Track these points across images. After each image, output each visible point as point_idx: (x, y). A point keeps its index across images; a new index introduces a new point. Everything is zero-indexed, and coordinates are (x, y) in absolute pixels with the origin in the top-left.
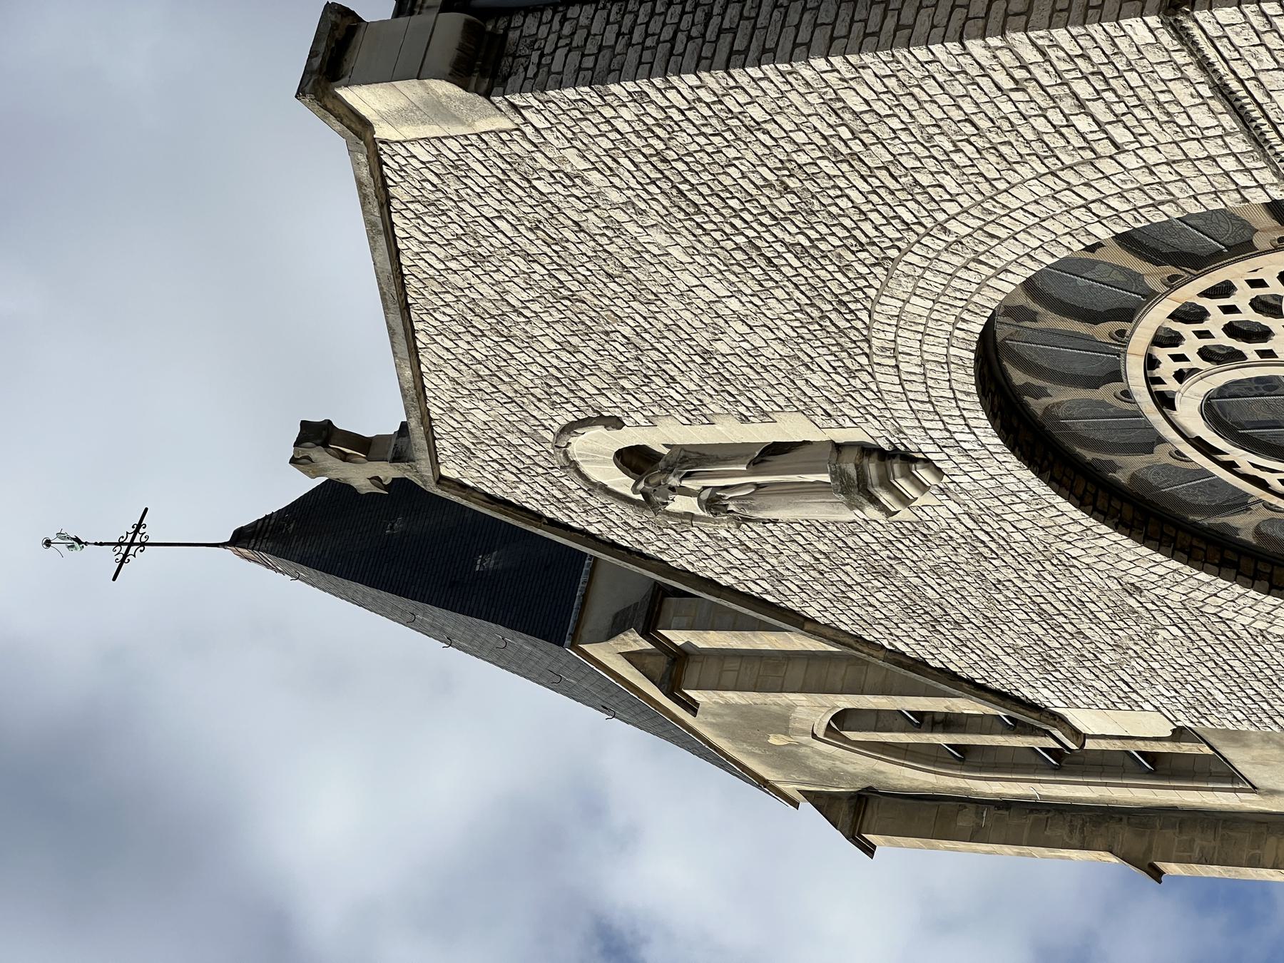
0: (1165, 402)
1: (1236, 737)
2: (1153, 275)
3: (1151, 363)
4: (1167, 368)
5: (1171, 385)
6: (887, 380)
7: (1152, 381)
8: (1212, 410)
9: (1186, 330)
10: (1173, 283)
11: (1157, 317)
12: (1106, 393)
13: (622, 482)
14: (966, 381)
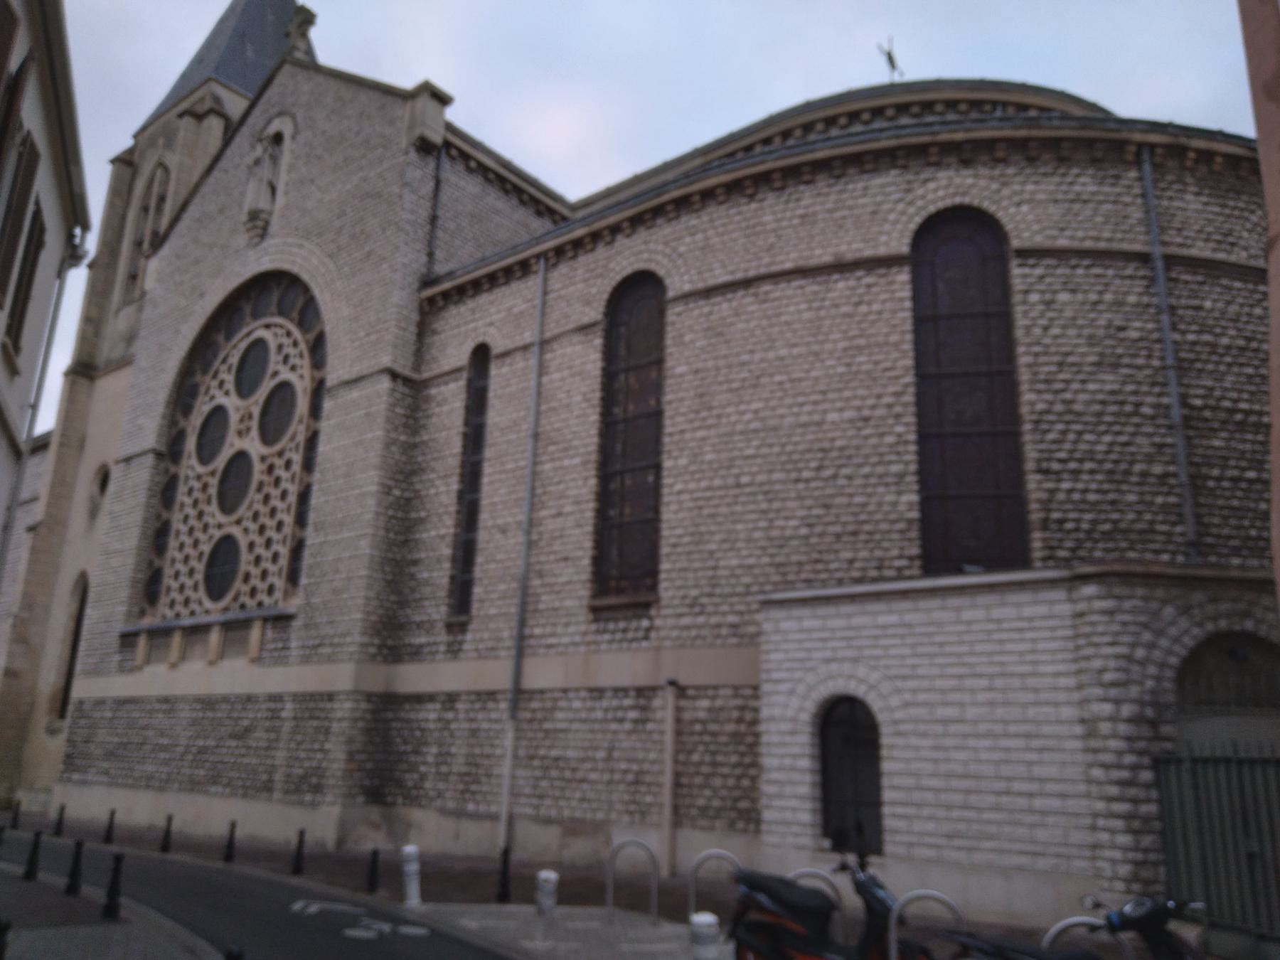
0: (268, 326)
1: (140, 309)
2: (311, 336)
3: (281, 327)
4: (279, 331)
5: (274, 330)
6: (291, 240)
7: (276, 325)
8: (260, 342)
9: (290, 341)
10: (307, 342)
11: (297, 333)
12: (273, 308)
13: (272, 130)
14: (286, 266)
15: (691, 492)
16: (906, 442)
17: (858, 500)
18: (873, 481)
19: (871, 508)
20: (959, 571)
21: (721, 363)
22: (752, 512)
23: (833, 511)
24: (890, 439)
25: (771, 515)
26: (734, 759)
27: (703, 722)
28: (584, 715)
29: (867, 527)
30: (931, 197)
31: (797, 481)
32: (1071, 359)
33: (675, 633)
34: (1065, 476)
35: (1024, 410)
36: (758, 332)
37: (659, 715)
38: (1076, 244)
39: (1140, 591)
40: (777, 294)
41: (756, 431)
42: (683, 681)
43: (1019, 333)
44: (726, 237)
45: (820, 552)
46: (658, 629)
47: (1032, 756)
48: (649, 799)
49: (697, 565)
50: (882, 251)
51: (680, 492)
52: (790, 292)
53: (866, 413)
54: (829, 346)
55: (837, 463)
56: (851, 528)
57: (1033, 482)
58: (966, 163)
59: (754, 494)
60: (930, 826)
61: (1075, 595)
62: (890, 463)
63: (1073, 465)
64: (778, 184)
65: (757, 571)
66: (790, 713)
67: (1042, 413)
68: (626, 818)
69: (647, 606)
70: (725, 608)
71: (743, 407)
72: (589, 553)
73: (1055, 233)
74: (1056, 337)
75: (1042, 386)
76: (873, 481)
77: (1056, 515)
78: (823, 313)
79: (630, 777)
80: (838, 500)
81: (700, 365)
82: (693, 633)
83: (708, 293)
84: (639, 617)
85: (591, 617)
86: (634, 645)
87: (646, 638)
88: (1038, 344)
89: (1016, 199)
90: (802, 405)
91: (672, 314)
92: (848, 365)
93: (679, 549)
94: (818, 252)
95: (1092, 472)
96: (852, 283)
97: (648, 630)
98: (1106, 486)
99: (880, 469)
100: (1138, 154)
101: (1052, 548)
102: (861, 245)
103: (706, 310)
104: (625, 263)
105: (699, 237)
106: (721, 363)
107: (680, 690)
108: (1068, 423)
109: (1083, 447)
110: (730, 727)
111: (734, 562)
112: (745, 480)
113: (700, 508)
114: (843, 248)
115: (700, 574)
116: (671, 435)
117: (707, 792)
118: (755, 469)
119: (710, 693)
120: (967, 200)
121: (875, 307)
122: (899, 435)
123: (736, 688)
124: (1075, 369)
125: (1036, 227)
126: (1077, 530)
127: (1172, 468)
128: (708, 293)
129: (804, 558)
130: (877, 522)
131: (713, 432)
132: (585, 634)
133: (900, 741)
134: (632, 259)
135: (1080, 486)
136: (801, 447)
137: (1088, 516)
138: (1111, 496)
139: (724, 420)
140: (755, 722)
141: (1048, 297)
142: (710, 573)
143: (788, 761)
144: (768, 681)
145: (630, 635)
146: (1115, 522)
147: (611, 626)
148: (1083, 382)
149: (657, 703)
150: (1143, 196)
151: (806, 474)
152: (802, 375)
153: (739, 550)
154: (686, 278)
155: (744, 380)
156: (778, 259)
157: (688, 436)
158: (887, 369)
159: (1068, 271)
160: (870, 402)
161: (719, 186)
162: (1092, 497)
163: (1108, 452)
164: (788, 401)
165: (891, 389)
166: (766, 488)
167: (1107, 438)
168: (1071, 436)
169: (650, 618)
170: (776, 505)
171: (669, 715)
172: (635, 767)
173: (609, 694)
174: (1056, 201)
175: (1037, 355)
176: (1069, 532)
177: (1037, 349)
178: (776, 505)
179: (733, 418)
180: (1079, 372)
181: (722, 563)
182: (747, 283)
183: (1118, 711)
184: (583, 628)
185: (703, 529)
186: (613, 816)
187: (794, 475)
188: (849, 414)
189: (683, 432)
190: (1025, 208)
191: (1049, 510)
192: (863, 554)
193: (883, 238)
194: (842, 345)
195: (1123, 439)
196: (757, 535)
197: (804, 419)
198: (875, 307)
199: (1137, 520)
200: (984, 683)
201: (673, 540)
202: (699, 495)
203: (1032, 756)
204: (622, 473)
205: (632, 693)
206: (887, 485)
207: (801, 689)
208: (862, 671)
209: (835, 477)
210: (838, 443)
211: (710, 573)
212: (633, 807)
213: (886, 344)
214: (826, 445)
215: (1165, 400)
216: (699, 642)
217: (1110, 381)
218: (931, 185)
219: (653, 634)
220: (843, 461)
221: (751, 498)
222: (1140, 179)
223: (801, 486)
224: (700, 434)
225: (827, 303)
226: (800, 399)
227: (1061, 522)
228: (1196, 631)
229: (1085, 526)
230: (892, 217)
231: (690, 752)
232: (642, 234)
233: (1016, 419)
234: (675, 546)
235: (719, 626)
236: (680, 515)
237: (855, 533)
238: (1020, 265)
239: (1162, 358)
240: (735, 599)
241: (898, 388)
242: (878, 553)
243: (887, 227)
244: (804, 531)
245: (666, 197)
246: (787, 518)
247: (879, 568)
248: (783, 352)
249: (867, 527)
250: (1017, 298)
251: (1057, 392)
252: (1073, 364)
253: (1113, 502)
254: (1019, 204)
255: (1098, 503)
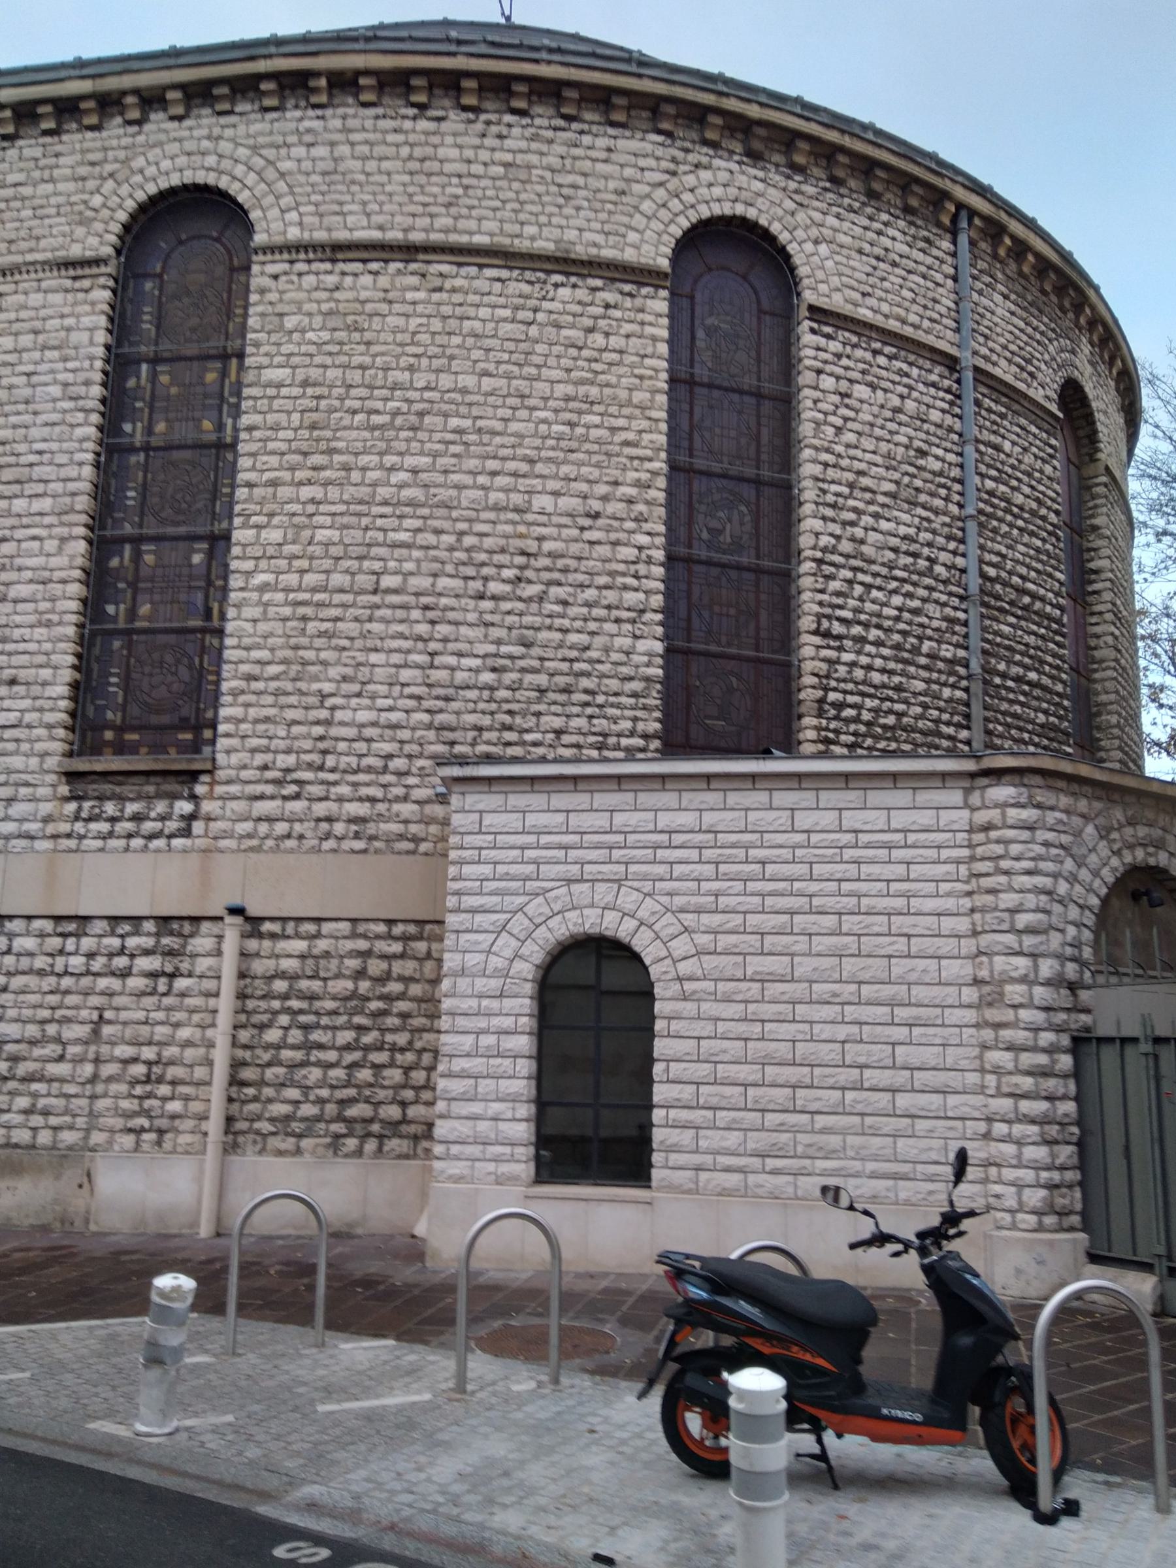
15: (287, 590)
16: (649, 561)
17: (573, 638)
18: (598, 612)
19: (593, 654)
20: (766, 753)
21: (356, 376)
22: (402, 636)
23: (536, 651)
24: (628, 553)
25: (433, 646)
26: (346, 1036)
27: (293, 977)
28: (40, 962)
29: (585, 683)
30: (703, 191)
31: (481, 597)
32: (865, 481)
33: (247, 826)
34: (848, 643)
35: (805, 541)
36: (424, 338)
37: (203, 964)
38: (879, 320)
39: (1064, 801)
40: (458, 282)
41: (410, 503)
42: (253, 910)
43: (806, 429)
44: (371, 166)
45: (510, 712)
46: (209, 819)
47: (901, 1033)
48: (175, 1106)
49: (290, 714)
50: (629, 255)
51: (263, 588)
52: (481, 284)
53: (596, 505)
54: (542, 387)
55: (546, 576)
56: (561, 680)
57: (808, 647)
58: (754, 157)
59: (405, 607)
60: (733, 1139)
61: (975, 799)
62: (625, 588)
63: (857, 630)
64: (469, 100)
65: (405, 734)
66: (495, 962)
67: (824, 550)
68: (128, 1140)
69: (193, 776)
70: (345, 790)
71: (389, 460)
72: (67, 675)
73: (857, 296)
74: (848, 446)
75: (829, 512)
76: (598, 612)
77: (832, 696)
78: (533, 331)
79: (139, 1070)
80: (544, 635)
81: (315, 373)
82: (281, 828)
83: (336, 251)
84: (174, 797)
85: (64, 790)
86: (160, 843)
87: (186, 833)
88: (828, 451)
89: (814, 232)
90: (494, 474)
91: (261, 274)
92: (571, 424)
93: (259, 685)
94: (531, 230)
95: (878, 643)
96: (582, 294)
97: (192, 817)
98: (892, 665)
99: (611, 596)
100: (955, 219)
101: (827, 741)
102: (599, 239)
103: (331, 280)
104: (166, 164)
105: (321, 151)
106: (356, 376)
107: (253, 924)
108: (855, 569)
109: (869, 606)
110: (344, 986)
111: (363, 716)
112: (388, 581)
113: (304, 619)
114: (571, 235)
115: (296, 730)
116: (250, 485)
117: (293, 1093)
118: (409, 566)
119: (311, 928)
120: (751, 213)
121: (615, 342)
122: (640, 548)
123: (390, 922)
124: (868, 496)
125: (835, 281)
126: (857, 720)
127: (961, 653)
128: (336, 251)
129: (486, 721)
130: (603, 676)
131: (333, 493)
132: (47, 820)
133: (689, 1008)
134: (182, 161)
135: (864, 660)
136: (488, 542)
137: (869, 703)
138: (896, 679)
139: (355, 476)
140: (435, 982)
141: (844, 386)
142: (318, 730)
143: (488, 1040)
144: (457, 910)
145: (149, 826)
146: (900, 715)
147: (110, 808)
148: (876, 516)
149: (202, 943)
150: (955, 279)
151: (494, 587)
152: (498, 426)
153: (373, 697)
154: (293, 216)
155: (396, 413)
156: (462, 224)
157: (284, 492)
158: (627, 443)
159: (868, 356)
160: (602, 489)
161: (367, 72)
162: (876, 677)
163: (897, 619)
164: (472, 463)
165: (632, 475)
166: (424, 600)
167: (897, 600)
168: (858, 590)
169: (193, 797)
170: (443, 629)
171: (229, 965)
172: (148, 1053)
173: (99, 926)
174: (860, 252)
175: (826, 465)
176: (848, 721)
177: (825, 457)
178: (443, 629)
179: (372, 475)
180: (870, 502)
181: (339, 715)
182: (409, 251)
183: (1036, 967)
184: (46, 808)
185: (310, 655)
186: (97, 1138)
187: (477, 585)
188: (565, 503)
189: (274, 483)
190: (823, 249)
191: (826, 689)
192: (581, 722)
193: (633, 237)
194: (561, 390)
195: (916, 604)
196: (406, 675)
197: (494, 497)
198: (615, 342)
199: (922, 717)
200: (829, 921)
201: (244, 668)
202: (306, 596)
203: (901, 1033)
204: (137, 541)
205: (149, 926)
206: (617, 621)
207: (519, 924)
208: (628, 899)
209: (541, 599)
210: (548, 546)
211: (318, 730)
212: (144, 1122)
213: (629, 403)
214: (532, 545)
215: (960, 562)
216: (290, 843)
217: (904, 522)
218: (705, 175)
219: (198, 827)
220: (556, 575)
221: (400, 614)
222: (954, 255)
223: (487, 605)
224: (306, 492)
225: (540, 317)
226: (492, 465)
227: (840, 706)
228: (1115, 862)
229: (866, 716)
230: (646, 206)
231: (262, 1027)
232: (204, 122)
233: (788, 551)
234: (250, 678)
235: (329, 820)
236: (262, 627)
237: (567, 690)
238: (813, 331)
239: (961, 506)
240: (362, 777)
241: (645, 476)
242: (600, 724)
243: (639, 221)
244: (487, 677)
245: (262, 66)
246: (460, 655)
247: (600, 747)
248: (469, 381)
249: (585, 683)
250: (807, 377)
251: (845, 524)
252: (866, 489)
253: (898, 688)
254: (816, 242)
255: (884, 686)
